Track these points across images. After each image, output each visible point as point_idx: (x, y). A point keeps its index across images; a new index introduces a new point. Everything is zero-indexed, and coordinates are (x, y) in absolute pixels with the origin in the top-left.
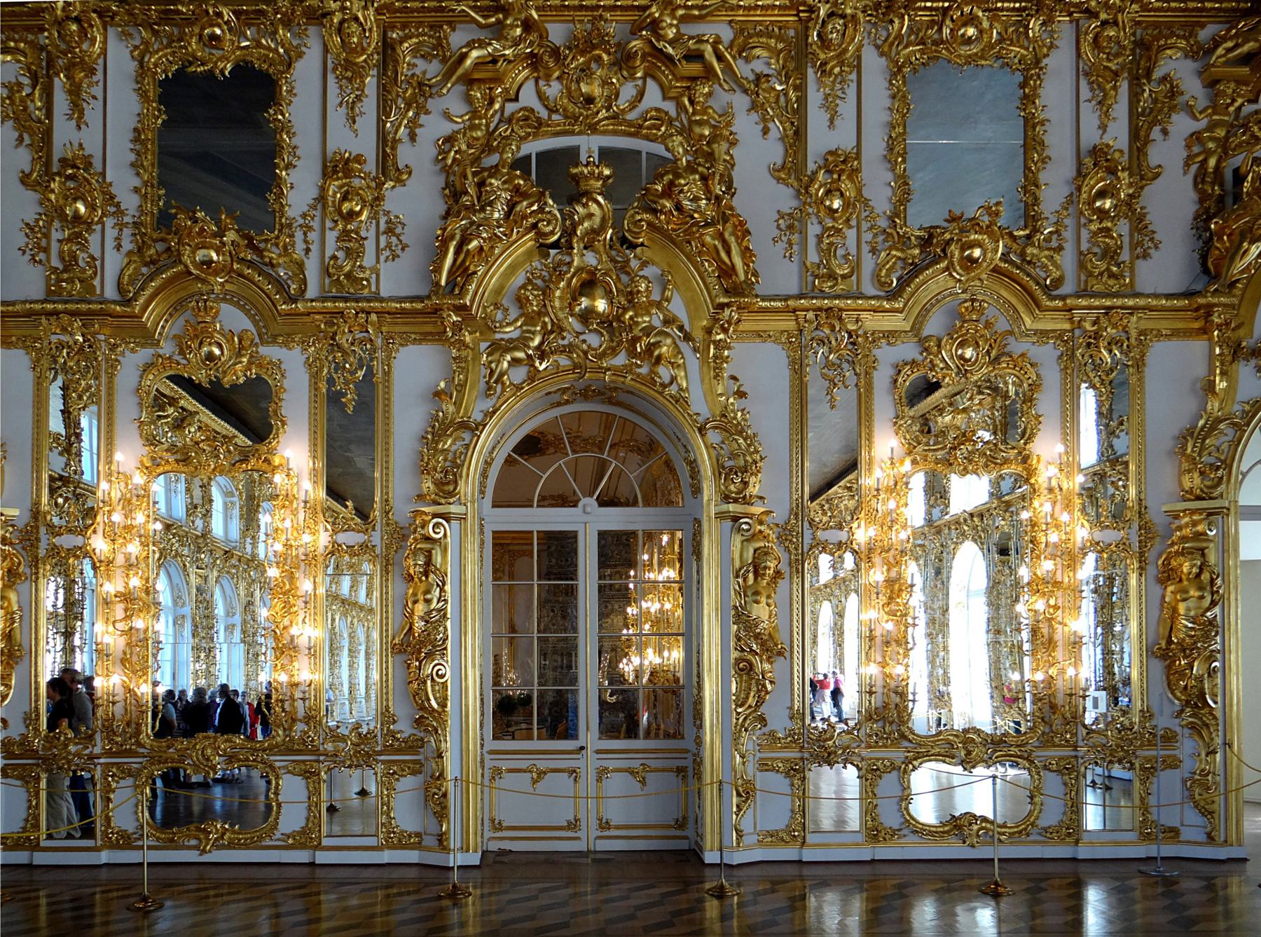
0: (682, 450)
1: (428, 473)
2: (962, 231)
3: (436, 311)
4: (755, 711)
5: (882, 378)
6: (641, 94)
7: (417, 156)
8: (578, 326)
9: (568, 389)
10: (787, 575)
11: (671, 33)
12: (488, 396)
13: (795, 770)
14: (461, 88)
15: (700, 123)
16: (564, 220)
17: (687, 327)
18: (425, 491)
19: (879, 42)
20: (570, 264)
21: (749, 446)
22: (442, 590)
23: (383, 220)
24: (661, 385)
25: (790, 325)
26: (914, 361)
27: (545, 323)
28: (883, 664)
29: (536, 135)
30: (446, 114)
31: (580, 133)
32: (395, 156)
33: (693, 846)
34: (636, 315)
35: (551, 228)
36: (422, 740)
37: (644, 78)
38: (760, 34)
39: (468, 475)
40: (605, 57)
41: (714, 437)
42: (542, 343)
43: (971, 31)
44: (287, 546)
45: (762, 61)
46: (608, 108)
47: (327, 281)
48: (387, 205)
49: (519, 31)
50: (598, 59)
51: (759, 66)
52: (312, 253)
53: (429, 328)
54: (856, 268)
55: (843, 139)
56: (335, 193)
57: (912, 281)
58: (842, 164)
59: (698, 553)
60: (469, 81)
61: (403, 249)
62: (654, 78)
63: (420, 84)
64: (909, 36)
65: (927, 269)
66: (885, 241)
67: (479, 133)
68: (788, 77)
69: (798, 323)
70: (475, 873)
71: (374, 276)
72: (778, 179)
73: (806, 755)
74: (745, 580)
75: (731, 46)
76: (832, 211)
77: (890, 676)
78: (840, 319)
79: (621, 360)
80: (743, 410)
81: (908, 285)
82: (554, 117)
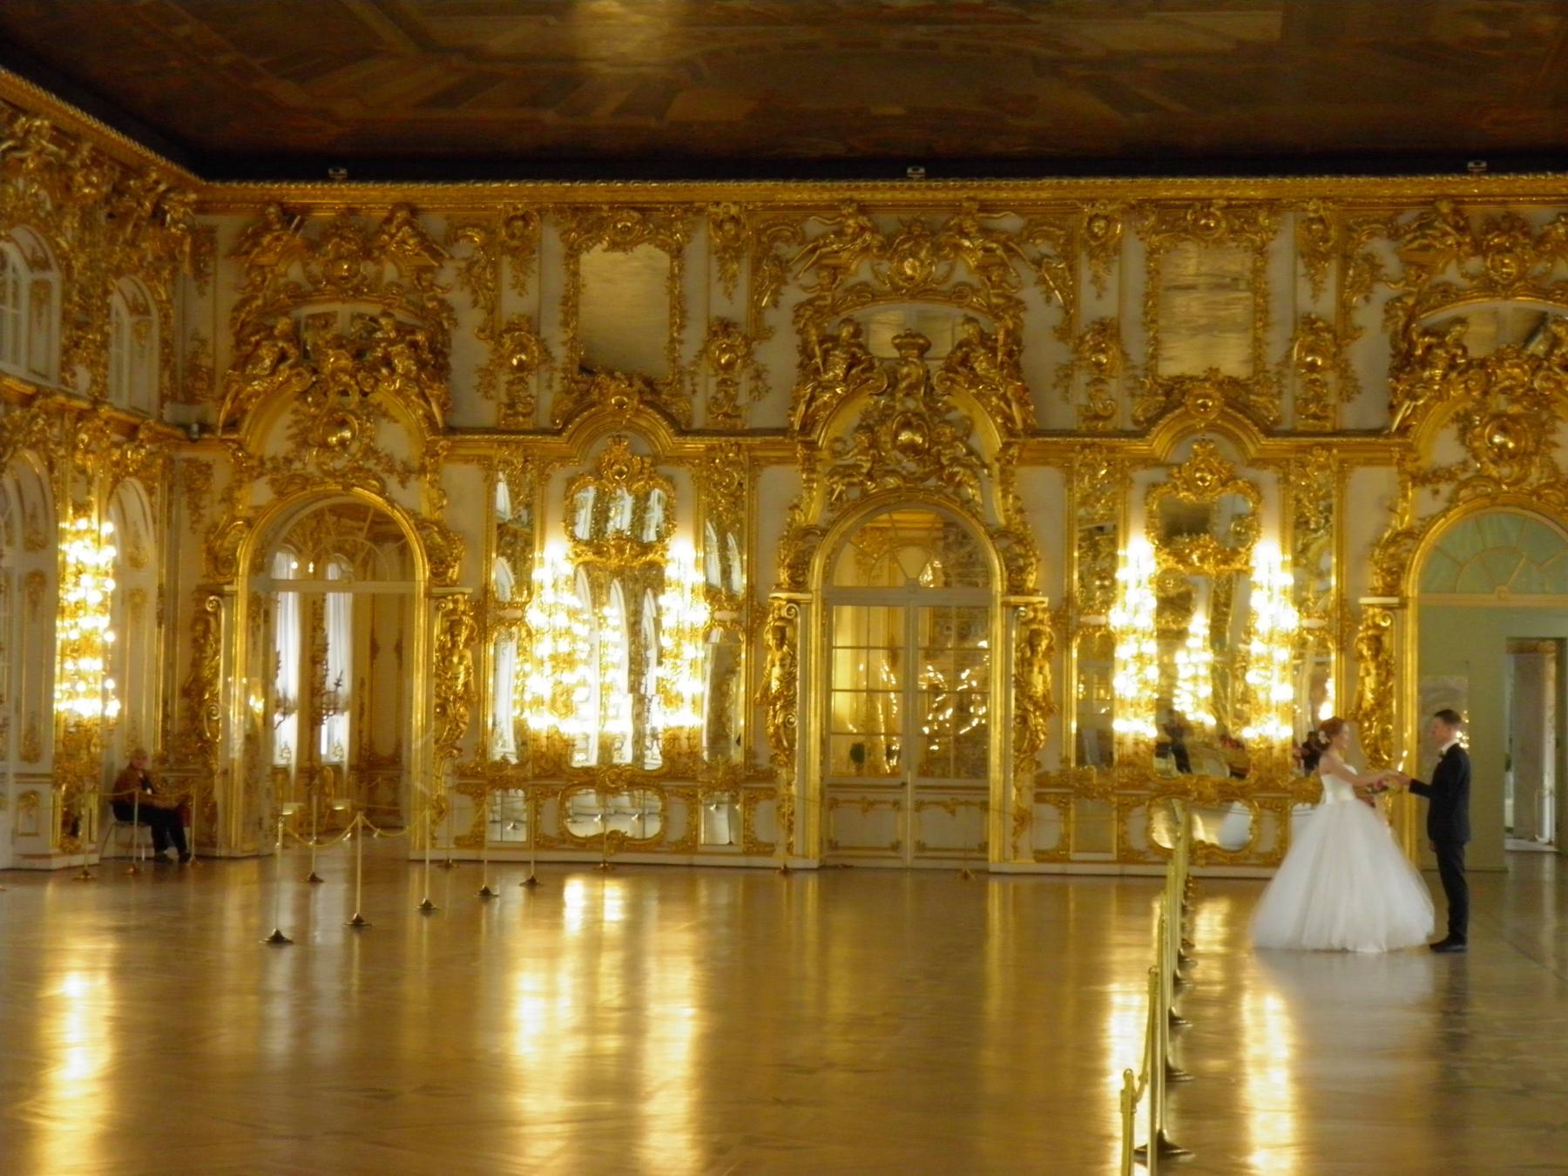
6: (952, 269)
7: (780, 319)
8: (900, 456)
48: (757, 358)
55: (1107, 308)
58: (1107, 330)
79: (932, 482)
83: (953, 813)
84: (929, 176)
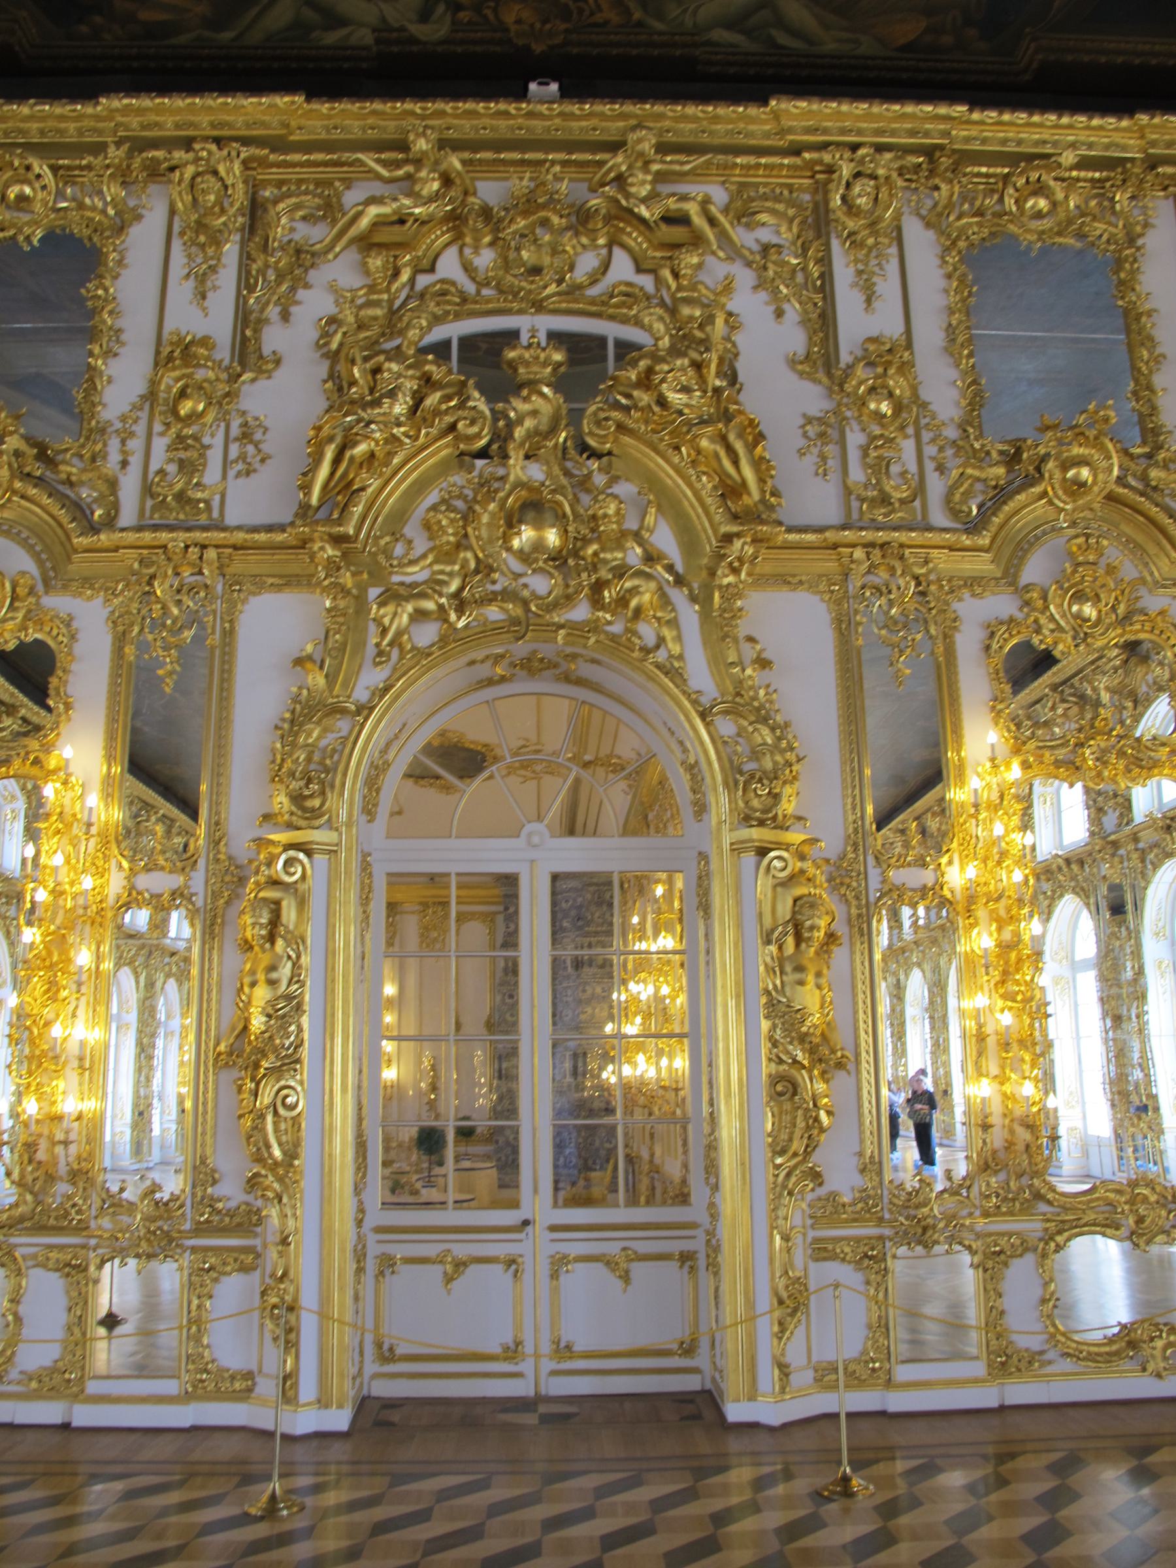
0: (675, 746)
1: (281, 781)
2: (1061, 443)
3: (303, 543)
4: (804, 1161)
5: (968, 642)
6: (606, 266)
7: (292, 338)
8: (515, 565)
9: (502, 656)
10: (845, 940)
11: (644, 191)
12: (376, 664)
13: (871, 1258)
14: (353, 255)
15: (688, 301)
16: (495, 420)
17: (679, 568)
18: (276, 808)
19: (924, 212)
20: (503, 479)
21: (779, 739)
22: (296, 965)
23: (235, 424)
24: (641, 649)
25: (831, 566)
26: (1011, 620)
27: (465, 562)
28: (1001, 1079)
29: (458, 316)
30: (336, 283)
31: (520, 312)
32: (258, 340)
33: (709, 1385)
34: (603, 549)
35: (475, 429)
36: (259, 1210)
37: (610, 246)
38: (765, 197)
39: (343, 784)
40: (556, 220)
41: (726, 727)
42: (461, 589)
43: (1042, 203)
44: (57, 893)
45: (771, 229)
46: (560, 282)
47: (149, 503)
49: (436, 186)
50: (545, 223)
51: (765, 235)
52: (133, 464)
53: (294, 569)
54: (920, 490)
56: (169, 388)
57: (998, 509)
58: (889, 356)
59: (705, 908)
60: (367, 243)
61: (263, 461)
62: (623, 246)
63: (298, 252)
64: (962, 205)
65: (1018, 492)
66: (956, 455)
67: (379, 312)
68: (805, 249)
69: (841, 565)
70: (338, 1451)
71: (217, 498)
72: (801, 374)
73: (887, 1232)
74: (780, 948)
75: (726, 210)
76: (879, 416)
77: (1012, 1097)
78: (901, 558)
79: (581, 612)
80: (768, 686)
81: (994, 514)
82: (485, 292)
83: (626, 1277)
84: (566, 94)
